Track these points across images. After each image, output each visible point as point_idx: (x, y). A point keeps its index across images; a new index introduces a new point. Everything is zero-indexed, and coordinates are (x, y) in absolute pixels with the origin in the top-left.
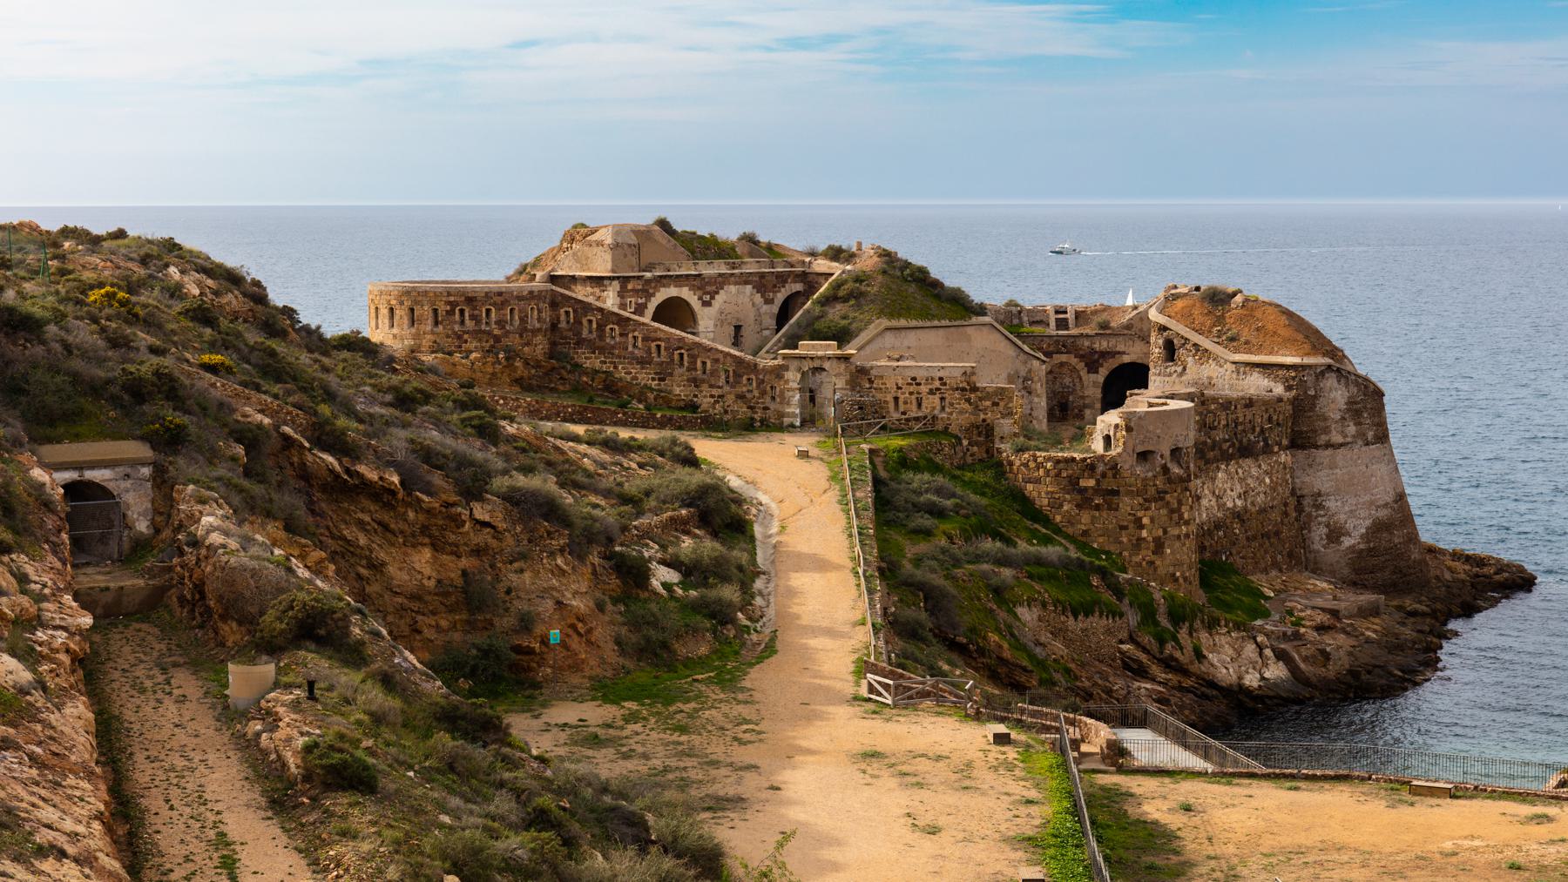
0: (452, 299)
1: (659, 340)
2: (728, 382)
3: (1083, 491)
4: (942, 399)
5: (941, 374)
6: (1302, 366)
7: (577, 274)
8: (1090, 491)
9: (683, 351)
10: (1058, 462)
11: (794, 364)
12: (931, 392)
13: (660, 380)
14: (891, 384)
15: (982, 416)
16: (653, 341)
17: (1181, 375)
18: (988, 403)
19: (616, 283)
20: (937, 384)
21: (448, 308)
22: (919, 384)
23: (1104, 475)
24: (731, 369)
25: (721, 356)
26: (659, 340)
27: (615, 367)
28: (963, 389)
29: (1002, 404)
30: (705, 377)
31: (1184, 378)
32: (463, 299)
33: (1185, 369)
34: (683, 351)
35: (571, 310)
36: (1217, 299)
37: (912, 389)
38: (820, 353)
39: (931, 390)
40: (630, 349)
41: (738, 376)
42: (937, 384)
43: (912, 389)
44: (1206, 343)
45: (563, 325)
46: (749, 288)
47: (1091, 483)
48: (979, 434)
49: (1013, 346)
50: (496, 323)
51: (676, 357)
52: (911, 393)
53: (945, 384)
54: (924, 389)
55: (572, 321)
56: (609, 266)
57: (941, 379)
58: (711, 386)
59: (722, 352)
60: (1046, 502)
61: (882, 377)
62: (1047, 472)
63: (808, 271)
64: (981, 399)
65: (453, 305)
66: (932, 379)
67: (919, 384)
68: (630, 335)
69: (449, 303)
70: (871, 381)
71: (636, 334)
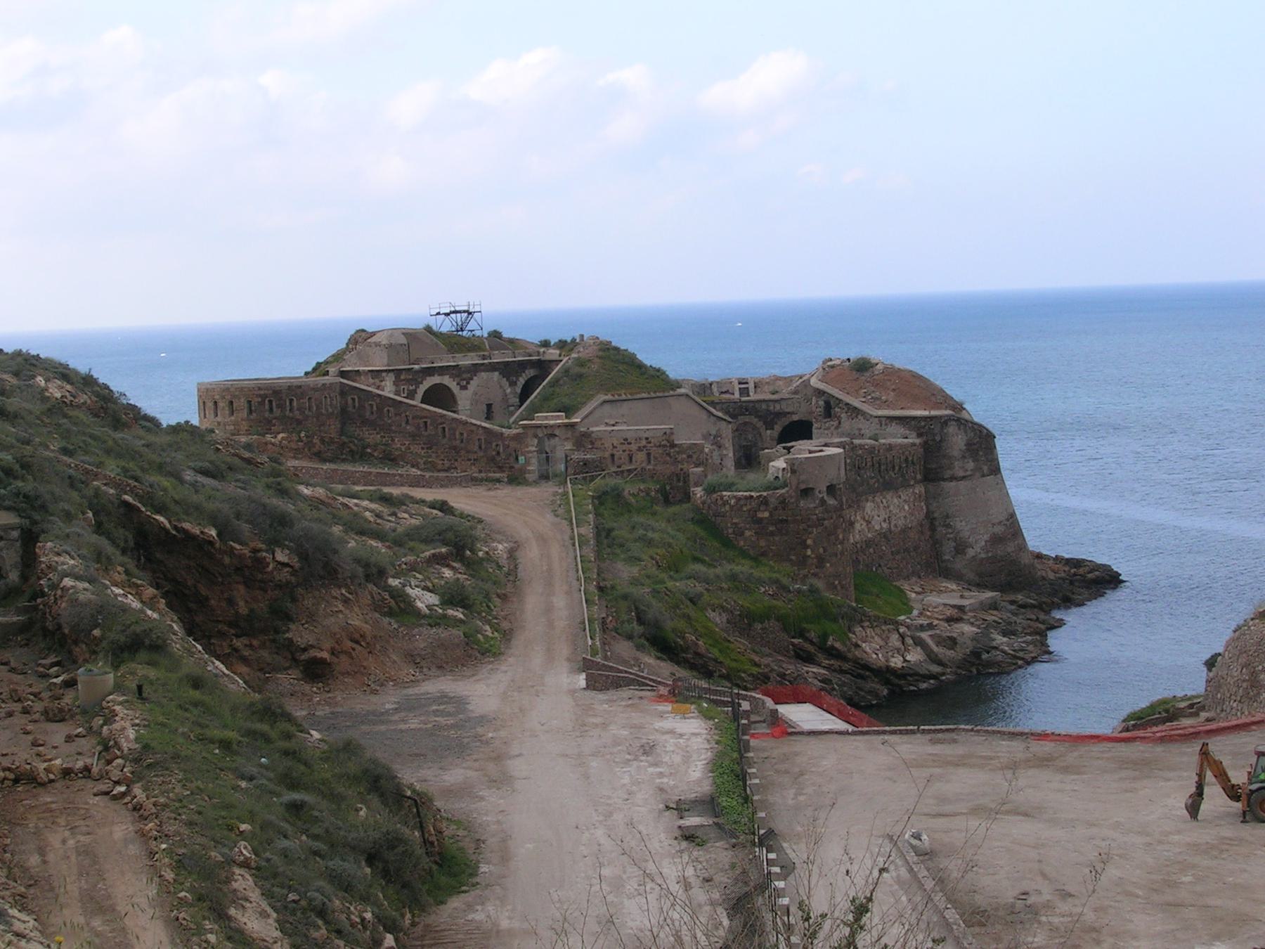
0: (262, 392)
1: (426, 417)
2: (480, 447)
3: (760, 521)
4: (649, 455)
5: (646, 436)
6: (929, 418)
7: (361, 369)
8: (765, 521)
9: (444, 425)
10: (738, 499)
11: (530, 432)
12: (640, 449)
13: (427, 448)
14: (608, 445)
15: (680, 466)
16: (421, 418)
17: (837, 428)
18: (684, 456)
19: (391, 375)
20: (644, 442)
21: (260, 400)
22: (630, 444)
23: (776, 509)
24: (483, 438)
25: (474, 428)
26: (426, 417)
27: (393, 440)
28: (665, 446)
29: (695, 456)
30: (463, 445)
31: (840, 430)
32: (271, 392)
33: (840, 423)
34: (444, 425)
35: (356, 397)
36: (863, 366)
37: (624, 447)
38: (552, 422)
39: (639, 447)
40: (404, 425)
41: (489, 443)
42: (644, 442)
43: (624, 447)
44: (855, 403)
45: (350, 409)
46: (496, 373)
47: (766, 514)
48: (679, 480)
49: (705, 412)
50: (298, 409)
51: (440, 430)
52: (624, 451)
53: (650, 443)
54: (634, 447)
55: (357, 405)
56: (385, 361)
57: (647, 439)
58: (468, 452)
59: (475, 425)
60: (730, 531)
61: (601, 439)
62: (732, 507)
63: (543, 358)
64: (678, 453)
65: (264, 397)
66: (640, 439)
67: (630, 444)
68: (403, 415)
69: (260, 396)
70: (592, 443)
71: (408, 413)
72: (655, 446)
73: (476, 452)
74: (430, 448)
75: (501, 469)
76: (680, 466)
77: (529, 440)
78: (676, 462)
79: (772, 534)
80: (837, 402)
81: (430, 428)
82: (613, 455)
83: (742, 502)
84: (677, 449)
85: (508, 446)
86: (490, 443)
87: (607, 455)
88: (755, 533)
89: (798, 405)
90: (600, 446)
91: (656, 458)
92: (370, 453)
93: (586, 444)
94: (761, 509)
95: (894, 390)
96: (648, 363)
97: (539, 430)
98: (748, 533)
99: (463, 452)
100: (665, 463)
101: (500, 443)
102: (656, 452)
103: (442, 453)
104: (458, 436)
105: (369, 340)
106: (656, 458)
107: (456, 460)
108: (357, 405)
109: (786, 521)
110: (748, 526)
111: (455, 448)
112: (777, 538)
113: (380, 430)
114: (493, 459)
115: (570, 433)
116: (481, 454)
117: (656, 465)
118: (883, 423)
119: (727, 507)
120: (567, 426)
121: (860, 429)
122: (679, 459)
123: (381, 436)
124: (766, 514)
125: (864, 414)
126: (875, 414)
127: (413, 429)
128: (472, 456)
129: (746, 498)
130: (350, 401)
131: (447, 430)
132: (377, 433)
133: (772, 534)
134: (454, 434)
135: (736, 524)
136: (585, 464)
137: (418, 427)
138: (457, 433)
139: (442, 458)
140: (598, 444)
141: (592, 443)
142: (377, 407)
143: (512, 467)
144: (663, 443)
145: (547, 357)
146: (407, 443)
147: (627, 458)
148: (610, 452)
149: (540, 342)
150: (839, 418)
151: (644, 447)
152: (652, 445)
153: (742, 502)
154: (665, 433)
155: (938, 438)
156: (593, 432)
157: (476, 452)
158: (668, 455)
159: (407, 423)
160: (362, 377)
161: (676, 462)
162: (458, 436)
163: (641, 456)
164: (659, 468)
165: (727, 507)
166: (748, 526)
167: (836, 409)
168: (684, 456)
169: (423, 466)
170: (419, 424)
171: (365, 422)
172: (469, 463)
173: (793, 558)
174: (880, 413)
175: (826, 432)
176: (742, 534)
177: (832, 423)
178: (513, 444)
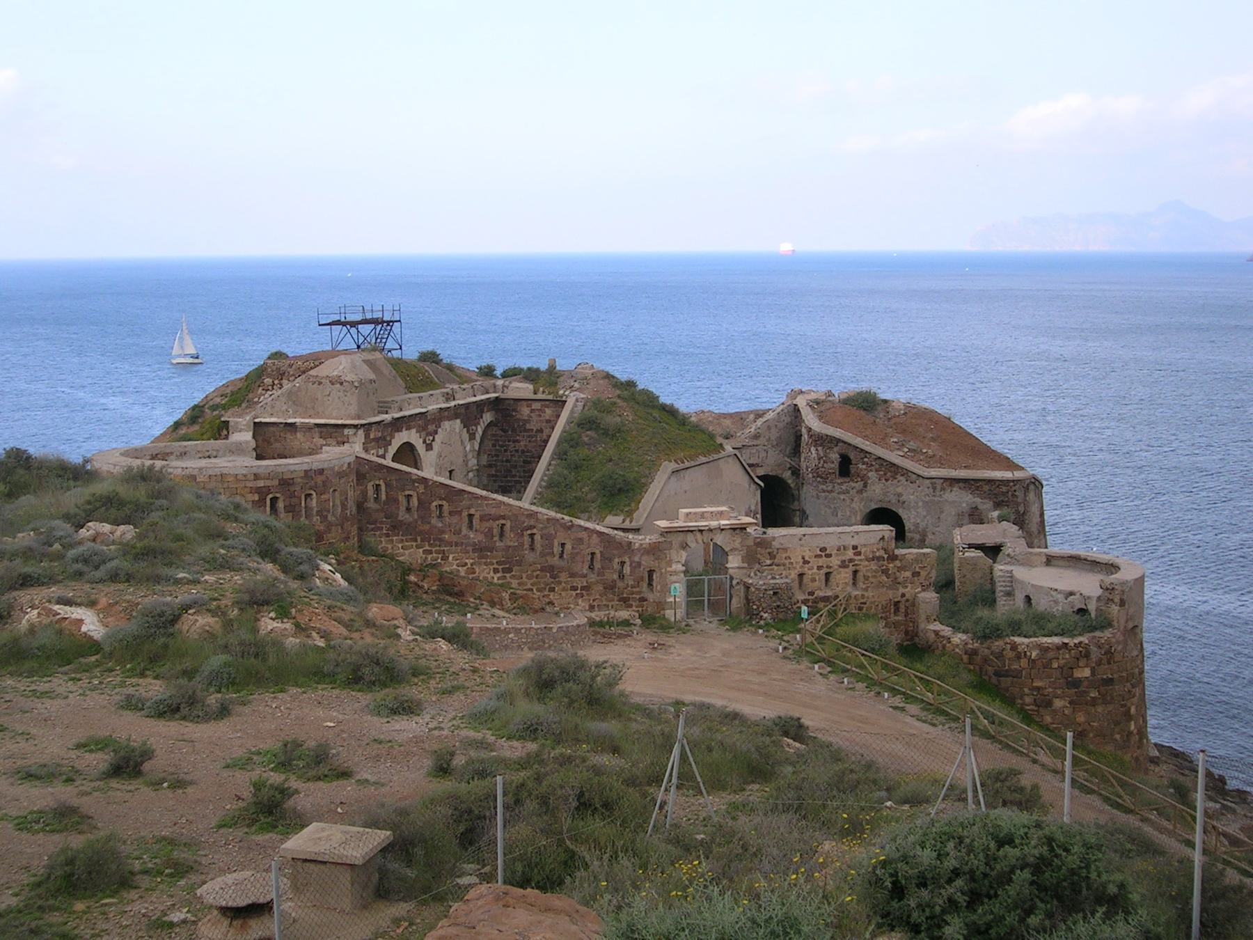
0: (261, 483)
1: (503, 517)
2: (591, 568)
3: (1076, 683)
4: (855, 572)
5: (854, 543)
6: (1013, 481)
7: (298, 420)
8: (1086, 683)
9: (535, 531)
10: (1044, 649)
11: (677, 540)
12: (844, 565)
13: (504, 571)
14: (796, 559)
15: (901, 590)
16: (494, 520)
17: (860, 492)
18: (908, 574)
19: (361, 432)
20: (850, 554)
21: (256, 497)
22: (829, 556)
23: (1099, 663)
24: (597, 552)
25: (584, 535)
26: (503, 517)
27: (445, 558)
28: (879, 558)
29: (923, 573)
30: (562, 563)
31: (865, 494)
32: (276, 482)
33: (865, 486)
34: (535, 531)
35: (381, 482)
36: (866, 404)
37: (821, 562)
38: (714, 524)
39: (843, 562)
40: (465, 531)
41: (607, 559)
42: (850, 554)
43: (821, 562)
44: (894, 457)
45: (371, 504)
46: (458, 421)
47: (1087, 673)
48: (897, 610)
49: (748, 477)
50: (319, 513)
51: (527, 539)
52: (819, 568)
53: (859, 554)
54: (835, 561)
55: (383, 497)
56: (353, 409)
57: (855, 547)
58: (572, 575)
59: (586, 529)
60: (1028, 700)
61: (785, 550)
62: (1032, 662)
63: (503, 396)
64: (900, 569)
65: (263, 492)
66: (845, 548)
67: (829, 556)
68: (465, 514)
69: (258, 490)
70: (772, 556)
71: (472, 511)
72: (867, 560)
73: (585, 576)
74: (509, 570)
75: (625, 602)
76: (901, 590)
77: (673, 552)
78: (896, 582)
79: (1094, 702)
80: (862, 455)
81: (508, 533)
82: (801, 575)
83: (1051, 655)
84: (898, 563)
85: (639, 564)
86: (610, 560)
87: (794, 575)
88: (1070, 703)
89: (765, 454)
90: (784, 561)
91: (866, 578)
92: (416, 584)
93: (763, 559)
94: (1081, 664)
95: (933, 439)
96: (686, 405)
97: (690, 537)
98: (1058, 703)
99: (563, 577)
100: (881, 585)
101: (627, 560)
102: (867, 568)
103: (529, 577)
104: (557, 549)
105: (312, 372)
106: (866, 578)
107: (552, 590)
108: (383, 497)
109: (1111, 680)
110: (1059, 692)
111: (551, 569)
112: (1100, 709)
113: (422, 540)
114: (611, 587)
115: (739, 540)
116: (593, 578)
117: (866, 590)
118: (939, 487)
119: (1024, 662)
120: (734, 529)
121: (900, 495)
122: (901, 579)
123: (424, 552)
124: (1087, 673)
125: (906, 472)
126: (926, 474)
127: (481, 537)
128: (580, 583)
129: (1058, 648)
130: (1001, 588)
131: (538, 537)
132: (418, 547)
133: (1094, 702)
134: (552, 547)
135: (1038, 689)
136: (775, 593)
137: (489, 534)
138: (556, 544)
139: (529, 586)
140: (781, 557)
141: (772, 556)
142: (419, 500)
143: (643, 599)
144: (877, 554)
145: (510, 394)
146: (469, 562)
147: (823, 578)
148: (799, 570)
149: (480, 369)
150: (864, 479)
151: (851, 560)
152: (862, 557)
153: (1051, 655)
154: (883, 538)
155: (1021, 509)
156: (774, 539)
157: (585, 576)
158: (885, 572)
159: (470, 526)
160: (299, 435)
161: (896, 582)
162: (557, 549)
163: (844, 576)
164: (870, 594)
165: (1024, 662)
166: (1059, 692)
167: (860, 466)
168: (908, 574)
169: (509, 604)
170: (491, 529)
171: (396, 527)
172: (574, 593)
173: (1118, 737)
174: (933, 472)
175: (842, 497)
176: (1049, 704)
177: (853, 485)
178: (647, 562)
